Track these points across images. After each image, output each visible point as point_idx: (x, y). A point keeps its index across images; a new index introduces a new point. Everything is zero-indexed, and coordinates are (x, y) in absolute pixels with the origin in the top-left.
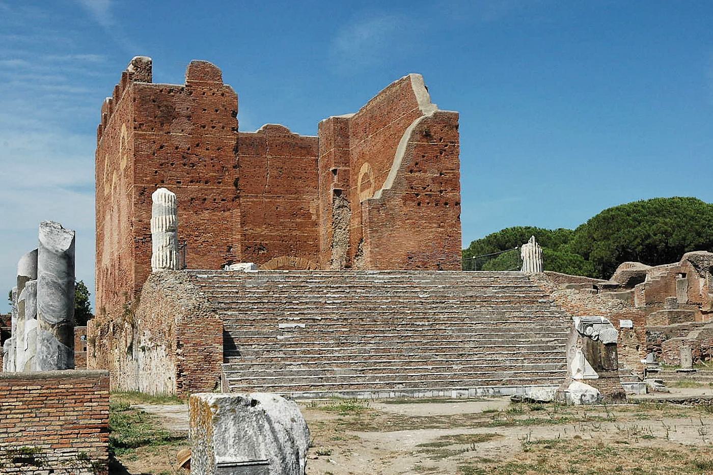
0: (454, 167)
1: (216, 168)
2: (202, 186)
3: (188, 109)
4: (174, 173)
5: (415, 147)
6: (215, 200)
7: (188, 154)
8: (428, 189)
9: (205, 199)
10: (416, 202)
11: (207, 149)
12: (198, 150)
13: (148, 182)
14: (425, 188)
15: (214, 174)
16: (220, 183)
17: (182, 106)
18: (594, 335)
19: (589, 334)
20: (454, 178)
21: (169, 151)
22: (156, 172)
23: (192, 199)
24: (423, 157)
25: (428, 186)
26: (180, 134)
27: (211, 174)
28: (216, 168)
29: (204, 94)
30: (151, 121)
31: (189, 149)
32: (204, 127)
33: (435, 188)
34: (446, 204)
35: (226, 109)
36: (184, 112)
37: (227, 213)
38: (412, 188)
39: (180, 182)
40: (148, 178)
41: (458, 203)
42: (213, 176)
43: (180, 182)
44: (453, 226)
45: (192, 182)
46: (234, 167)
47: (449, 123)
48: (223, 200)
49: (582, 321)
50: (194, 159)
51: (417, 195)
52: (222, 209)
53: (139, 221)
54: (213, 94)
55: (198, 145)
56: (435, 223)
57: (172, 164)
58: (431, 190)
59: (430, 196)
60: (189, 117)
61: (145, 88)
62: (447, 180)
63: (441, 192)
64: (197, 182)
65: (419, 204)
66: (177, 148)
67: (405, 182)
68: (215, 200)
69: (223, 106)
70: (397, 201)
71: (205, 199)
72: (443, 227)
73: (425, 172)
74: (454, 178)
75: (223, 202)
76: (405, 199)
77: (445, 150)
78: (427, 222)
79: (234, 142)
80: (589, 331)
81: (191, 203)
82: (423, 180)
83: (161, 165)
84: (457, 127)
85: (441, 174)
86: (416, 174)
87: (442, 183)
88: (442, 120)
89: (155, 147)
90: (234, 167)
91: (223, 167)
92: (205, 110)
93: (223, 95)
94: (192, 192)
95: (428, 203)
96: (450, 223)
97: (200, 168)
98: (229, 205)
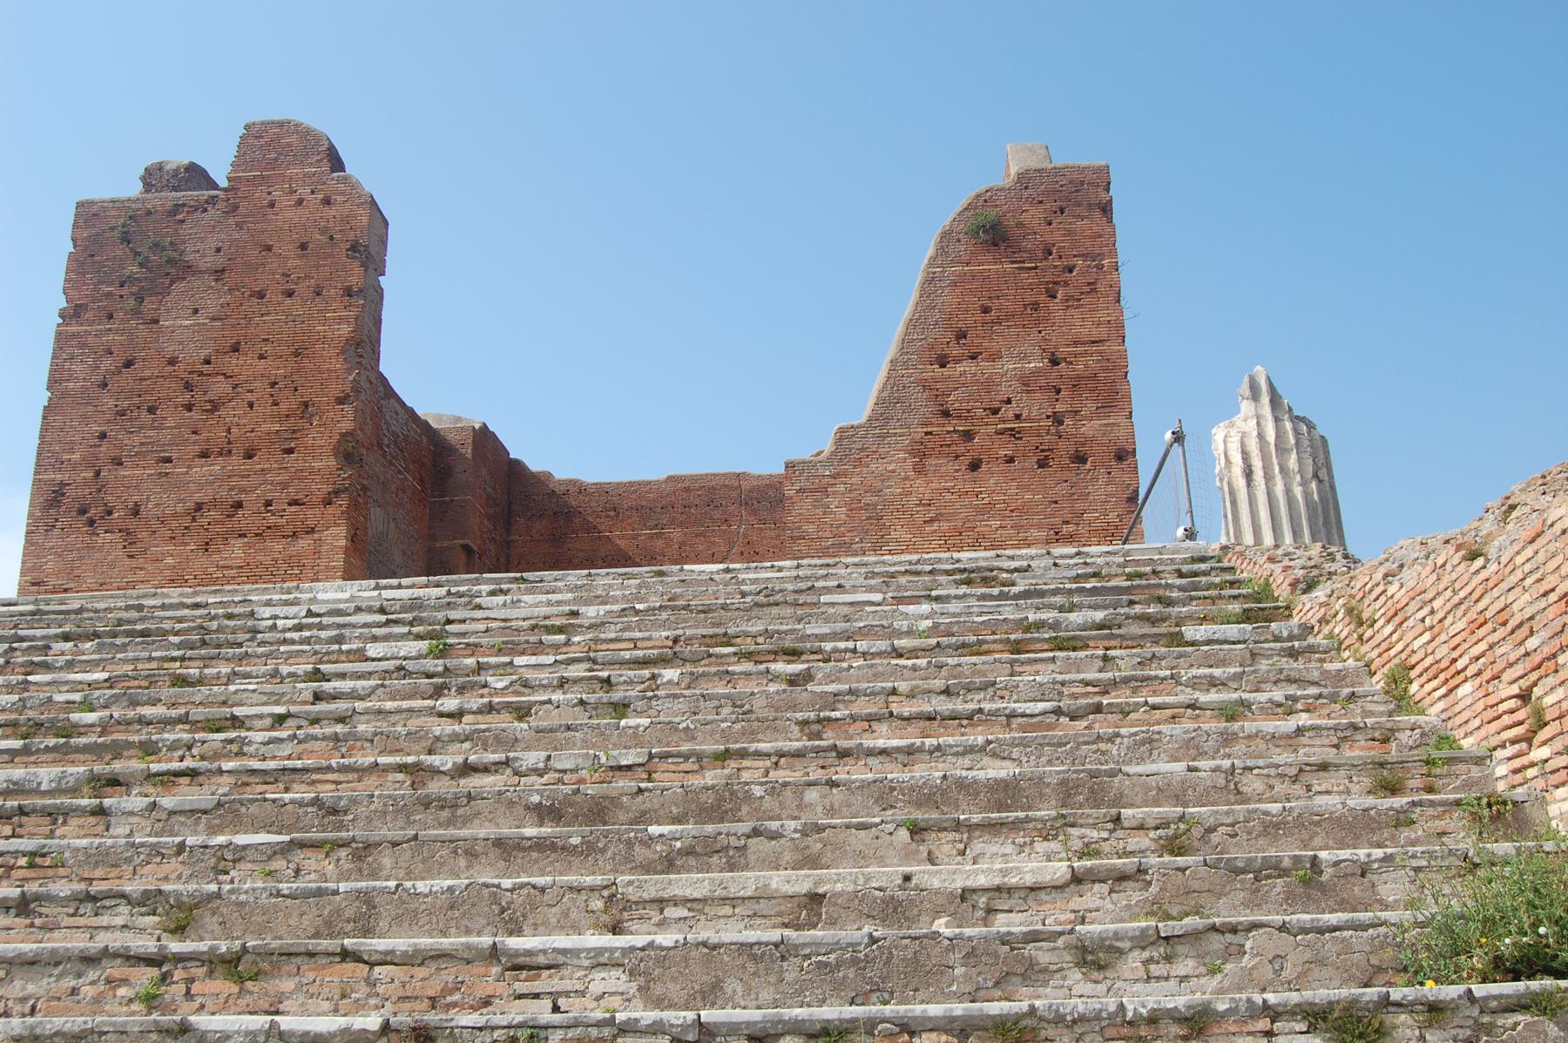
0: (1096, 333)
1: (284, 407)
2: (236, 462)
3: (218, 250)
4: (152, 433)
5: (955, 284)
6: (268, 503)
7: (201, 374)
8: (1009, 412)
9: (239, 505)
10: (965, 461)
11: (261, 357)
12: (233, 363)
13: (75, 466)
14: (995, 411)
15: (277, 427)
16: (290, 451)
17: (203, 242)
20: (1105, 369)
21: (147, 373)
22: (103, 436)
23: (199, 507)
24: (986, 310)
26: (184, 326)
27: (265, 427)
28: (284, 407)
29: (272, 205)
30: (109, 295)
31: (208, 362)
32: (261, 295)
33: (1035, 407)
34: (1080, 459)
35: (331, 238)
36: (208, 261)
37: (304, 543)
39: (169, 460)
40: (76, 456)
43: (169, 460)
45: (204, 455)
46: (340, 401)
47: (1080, 197)
48: (295, 503)
50: (220, 387)
51: (968, 436)
52: (289, 530)
53: (33, 584)
54: (300, 202)
55: (235, 349)
56: (1039, 527)
57: (152, 410)
58: (1018, 417)
60: (219, 273)
61: (105, 209)
62: (1079, 377)
63: (1058, 419)
64: (221, 454)
65: (975, 466)
66: (172, 362)
67: (920, 397)
68: (268, 503)
69: (323, 231)
70: (897, 460)
71: (239, 505)
72: (1070, 539)
73: (995, 357)
74: (1105, 369)
75: (293, 509)
76: (920, 453)
77: (1066, 284)
78: (1009, 523)
79: (346, 329)
81: (194, 519)
82: (989, 385)
83: (122, 413)
84: (1106, 209)
85: (1054, 362)
86: (966, 367)
87: (1058, 391)
88: (1048, 193)
89: (107, 364)
90: (340, 401)
91: (306, 405)
92: (269, 248)
93: (327, 202)
94: (201, 486)
95: (1011, 460)
97: (233, 413)
98: (312, 516)
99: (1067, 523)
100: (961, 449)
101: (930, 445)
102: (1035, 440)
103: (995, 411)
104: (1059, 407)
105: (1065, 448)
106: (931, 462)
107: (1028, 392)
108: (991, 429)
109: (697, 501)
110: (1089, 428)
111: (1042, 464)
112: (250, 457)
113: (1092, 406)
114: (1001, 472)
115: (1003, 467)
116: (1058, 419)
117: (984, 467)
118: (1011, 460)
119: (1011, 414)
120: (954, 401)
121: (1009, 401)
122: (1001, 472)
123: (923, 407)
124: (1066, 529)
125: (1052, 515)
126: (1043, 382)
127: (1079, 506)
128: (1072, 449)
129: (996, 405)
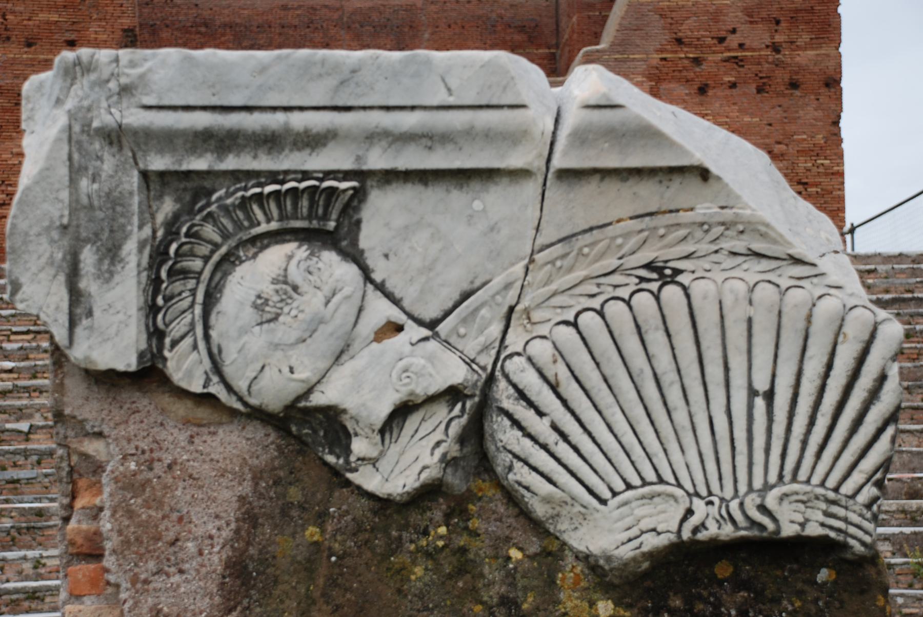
8: (733, 41)
14: (722, 40)
15: (54, 17)
18: (361, 388)
19: (273, 391)
25: (734, 31)
27: (43, 16)
33: (757, 37)
34: (794, 85)
38: (679, 41)
41: (832, 82)
42: (48, 23)
44: (815, 152)
49: (115, 137)
58: (741, 46)
59: (737, 61)
62: (797, 11)
80: (279, 320)
87: (778, 22)
95: (733, 85)
96: (805, 145)
99: (779, 143)
100: (691, 75)
101: (665, 70)
102: (755, 68)
103: (722, 40)
104: (778, 38)
105: (782, 76)
106: (664, 86)
107: (751, 22)
108: (719, 57)
109: (296, 22)
110: (805, 57)
111: (760, 90)
112: (29, 45)
113: (806, 37)
114: (726, 97)
115: (728, 92)
116: (776, 48)
117: (710, 93)
118: (733, 85)
119: (735, 44)
120: (686, 29)
121: (734, 31)
122: (726, 97)
123: (659, 36)
124: (778, 148)
125: (767, 136)
126: (764, 14)
127: (793, 128)
128: (787, 77)
129: (723, 34)
